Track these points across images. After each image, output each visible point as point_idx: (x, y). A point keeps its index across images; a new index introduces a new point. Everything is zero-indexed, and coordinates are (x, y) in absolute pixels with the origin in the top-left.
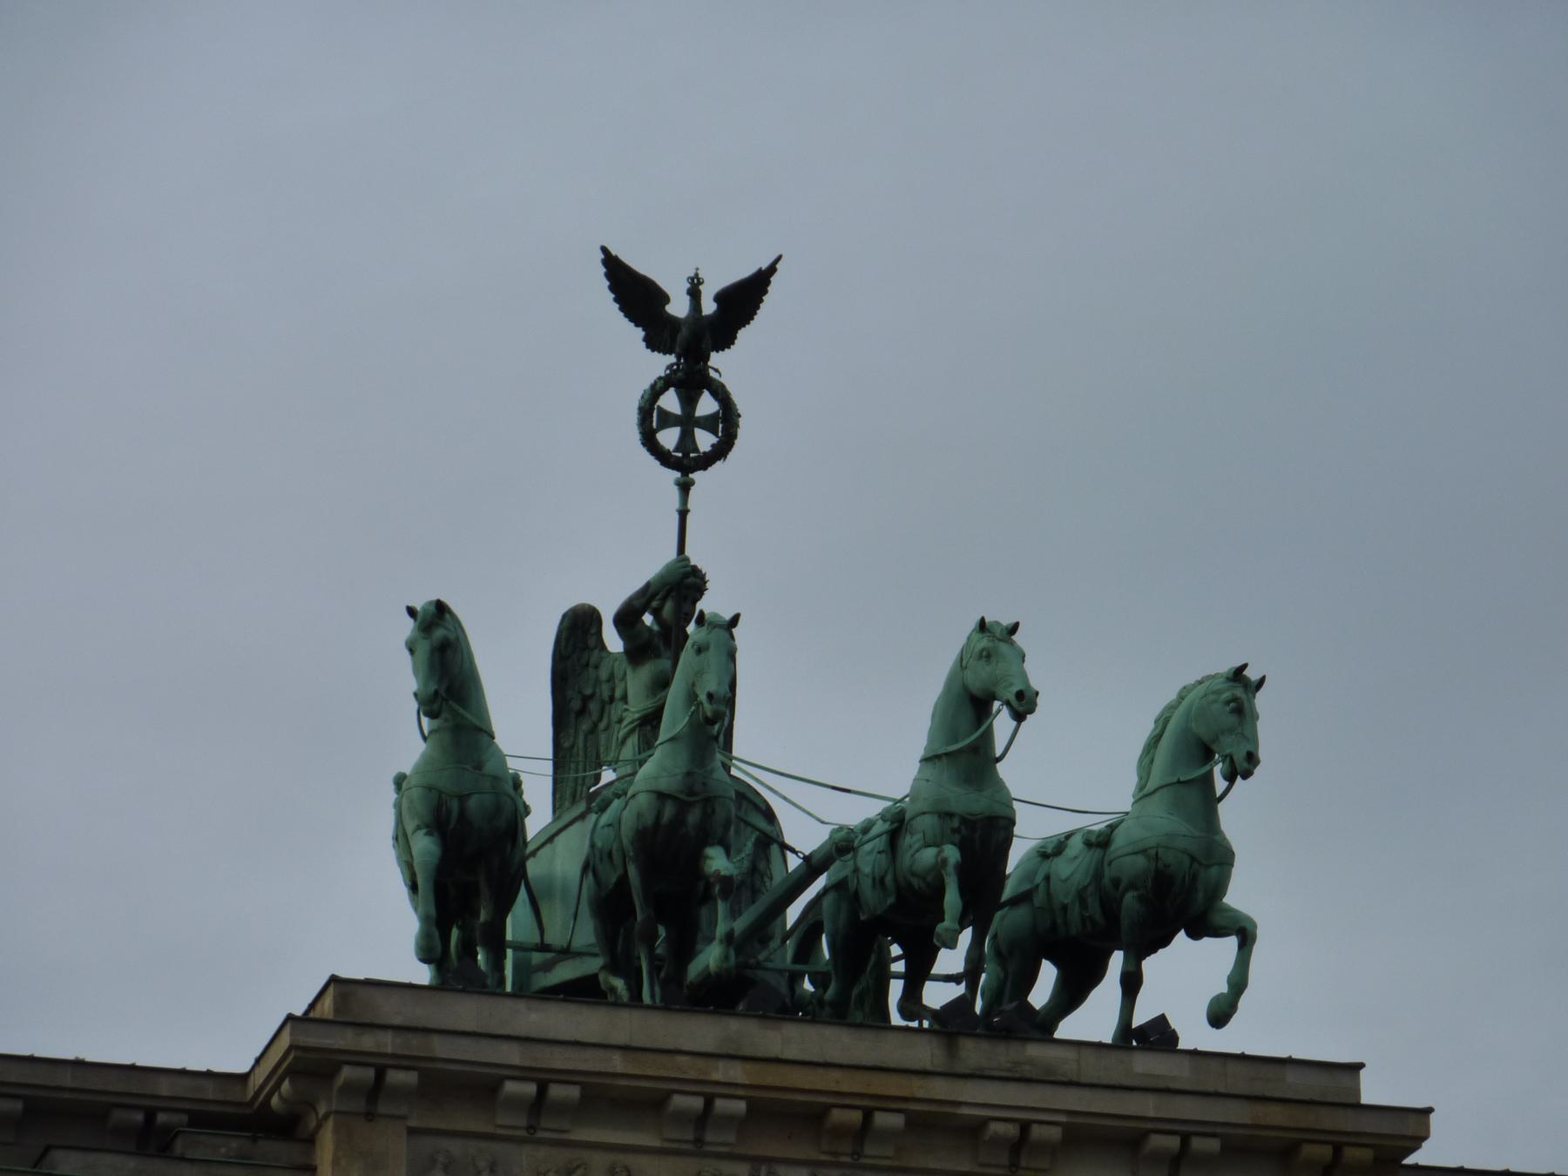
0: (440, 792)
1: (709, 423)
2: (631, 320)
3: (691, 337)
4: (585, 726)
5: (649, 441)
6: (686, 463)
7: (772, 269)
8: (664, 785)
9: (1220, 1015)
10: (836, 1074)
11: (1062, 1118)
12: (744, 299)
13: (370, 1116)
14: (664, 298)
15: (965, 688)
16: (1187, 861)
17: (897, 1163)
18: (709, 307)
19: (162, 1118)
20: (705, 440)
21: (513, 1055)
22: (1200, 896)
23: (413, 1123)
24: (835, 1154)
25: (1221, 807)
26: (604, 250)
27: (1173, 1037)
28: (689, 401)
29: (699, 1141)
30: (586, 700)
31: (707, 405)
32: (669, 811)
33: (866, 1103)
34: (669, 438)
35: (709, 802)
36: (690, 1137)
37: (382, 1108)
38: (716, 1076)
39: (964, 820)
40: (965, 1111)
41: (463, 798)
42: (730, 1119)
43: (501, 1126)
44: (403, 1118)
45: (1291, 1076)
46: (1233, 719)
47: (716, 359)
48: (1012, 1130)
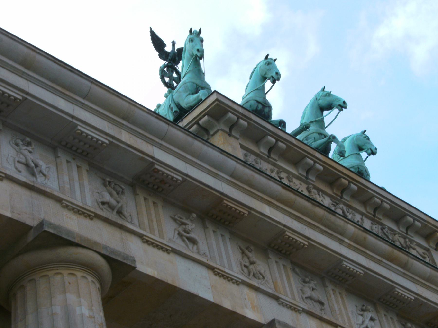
0: (197, 85)
2: (156, 49)
5: (162, 78)
8: (258, 99)
13: (230, 135)
14: (164, 45)
15: (318, 105)
17: (350, 204)
23: (240, 142)
26: (151, 28)
40: (369, 191)
42: (318, 170)
43: (261, 152)
44: (238, 139)
46: (368, 141)
48: (379, 201)
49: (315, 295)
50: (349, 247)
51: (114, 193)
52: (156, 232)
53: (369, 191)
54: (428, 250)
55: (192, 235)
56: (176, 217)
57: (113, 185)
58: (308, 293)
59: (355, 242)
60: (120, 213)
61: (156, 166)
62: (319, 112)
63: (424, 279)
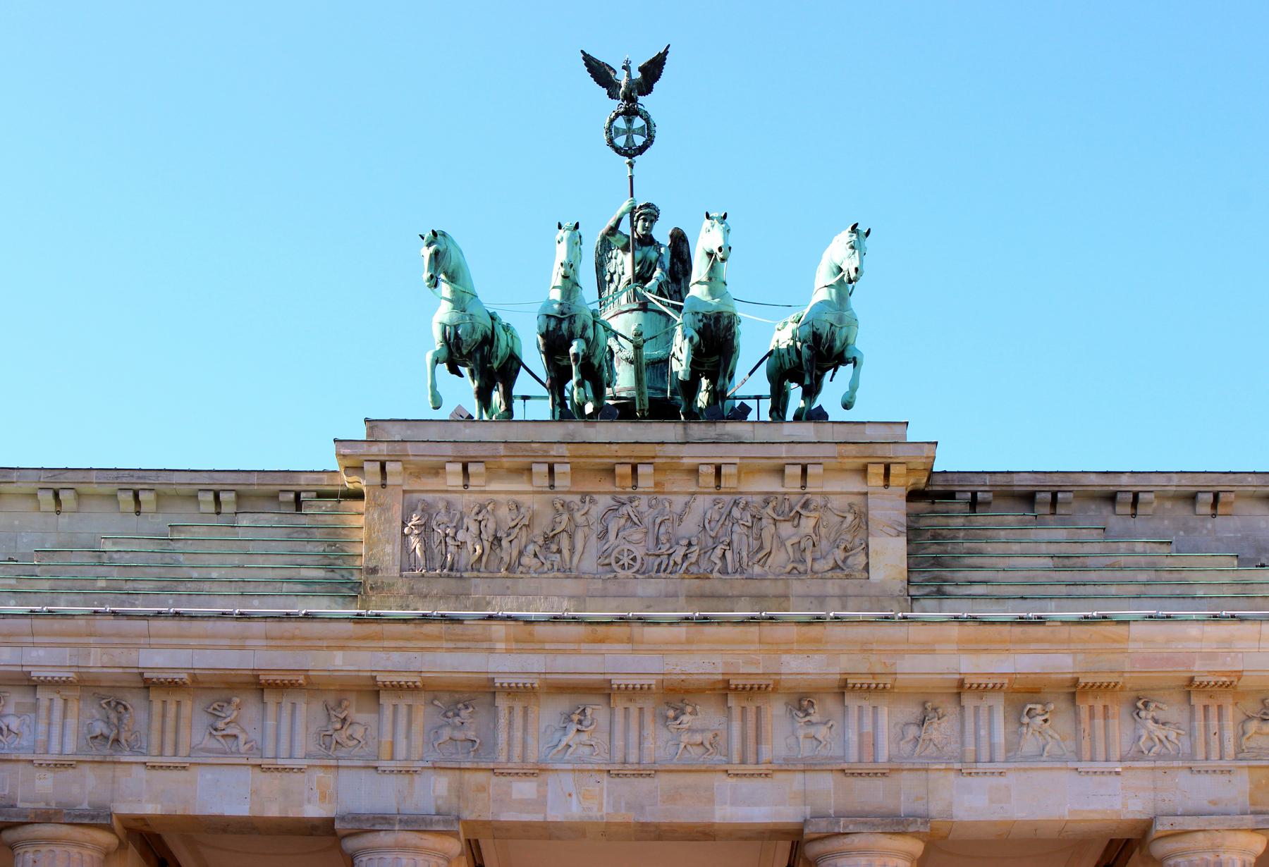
1: (641, 131)
3: (631, 90)
4: (613, 286)
5: (611, 142)
6: (631, 152)
7: (666, 52)
9: (847, 406)
10: (615, 447)
11: (737, 461)
12: (653, 70)
16: (828, 326)
18: (637, 75)
19: (303, 495)
20: (639, 140)
21: (448, 450)
22: (838, 343)
24: (623, 487)
25: (852, 298)
27: (825, 416)
28: (629, 121)
29: (552, 486)
30: (612, 275)
31: (638, 122)
32: (553, 324)
33: (632, 461)
34: (620, 141)
35: (572, 318)
36: (546, 482)
37: (390, 481)
38: (553, 453)
39: (704, 315)
40: (685, 461)
41: (456, 327)
45: (868, 429)
46: (851, 251)
47: (641, 99)
49: (459, 735)
50: (509, 651)
51: (113, 716)
52: (169, 750)
53: (685, 461)
54: (866, 494)
55: (229, 731)
56: (210, 710)
57: (113, 704)
58: (446, 733)
59: (517, 641)
60: (117, 741)
61: (146, 675)
62: (706, 259)
63: (682, 643)
